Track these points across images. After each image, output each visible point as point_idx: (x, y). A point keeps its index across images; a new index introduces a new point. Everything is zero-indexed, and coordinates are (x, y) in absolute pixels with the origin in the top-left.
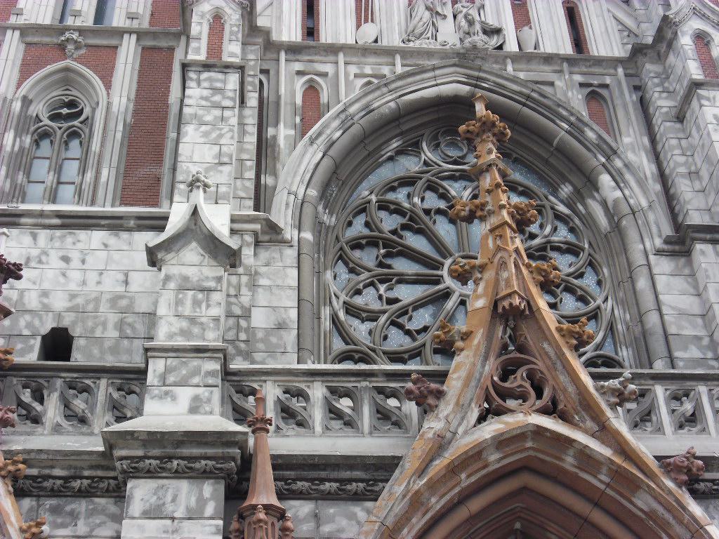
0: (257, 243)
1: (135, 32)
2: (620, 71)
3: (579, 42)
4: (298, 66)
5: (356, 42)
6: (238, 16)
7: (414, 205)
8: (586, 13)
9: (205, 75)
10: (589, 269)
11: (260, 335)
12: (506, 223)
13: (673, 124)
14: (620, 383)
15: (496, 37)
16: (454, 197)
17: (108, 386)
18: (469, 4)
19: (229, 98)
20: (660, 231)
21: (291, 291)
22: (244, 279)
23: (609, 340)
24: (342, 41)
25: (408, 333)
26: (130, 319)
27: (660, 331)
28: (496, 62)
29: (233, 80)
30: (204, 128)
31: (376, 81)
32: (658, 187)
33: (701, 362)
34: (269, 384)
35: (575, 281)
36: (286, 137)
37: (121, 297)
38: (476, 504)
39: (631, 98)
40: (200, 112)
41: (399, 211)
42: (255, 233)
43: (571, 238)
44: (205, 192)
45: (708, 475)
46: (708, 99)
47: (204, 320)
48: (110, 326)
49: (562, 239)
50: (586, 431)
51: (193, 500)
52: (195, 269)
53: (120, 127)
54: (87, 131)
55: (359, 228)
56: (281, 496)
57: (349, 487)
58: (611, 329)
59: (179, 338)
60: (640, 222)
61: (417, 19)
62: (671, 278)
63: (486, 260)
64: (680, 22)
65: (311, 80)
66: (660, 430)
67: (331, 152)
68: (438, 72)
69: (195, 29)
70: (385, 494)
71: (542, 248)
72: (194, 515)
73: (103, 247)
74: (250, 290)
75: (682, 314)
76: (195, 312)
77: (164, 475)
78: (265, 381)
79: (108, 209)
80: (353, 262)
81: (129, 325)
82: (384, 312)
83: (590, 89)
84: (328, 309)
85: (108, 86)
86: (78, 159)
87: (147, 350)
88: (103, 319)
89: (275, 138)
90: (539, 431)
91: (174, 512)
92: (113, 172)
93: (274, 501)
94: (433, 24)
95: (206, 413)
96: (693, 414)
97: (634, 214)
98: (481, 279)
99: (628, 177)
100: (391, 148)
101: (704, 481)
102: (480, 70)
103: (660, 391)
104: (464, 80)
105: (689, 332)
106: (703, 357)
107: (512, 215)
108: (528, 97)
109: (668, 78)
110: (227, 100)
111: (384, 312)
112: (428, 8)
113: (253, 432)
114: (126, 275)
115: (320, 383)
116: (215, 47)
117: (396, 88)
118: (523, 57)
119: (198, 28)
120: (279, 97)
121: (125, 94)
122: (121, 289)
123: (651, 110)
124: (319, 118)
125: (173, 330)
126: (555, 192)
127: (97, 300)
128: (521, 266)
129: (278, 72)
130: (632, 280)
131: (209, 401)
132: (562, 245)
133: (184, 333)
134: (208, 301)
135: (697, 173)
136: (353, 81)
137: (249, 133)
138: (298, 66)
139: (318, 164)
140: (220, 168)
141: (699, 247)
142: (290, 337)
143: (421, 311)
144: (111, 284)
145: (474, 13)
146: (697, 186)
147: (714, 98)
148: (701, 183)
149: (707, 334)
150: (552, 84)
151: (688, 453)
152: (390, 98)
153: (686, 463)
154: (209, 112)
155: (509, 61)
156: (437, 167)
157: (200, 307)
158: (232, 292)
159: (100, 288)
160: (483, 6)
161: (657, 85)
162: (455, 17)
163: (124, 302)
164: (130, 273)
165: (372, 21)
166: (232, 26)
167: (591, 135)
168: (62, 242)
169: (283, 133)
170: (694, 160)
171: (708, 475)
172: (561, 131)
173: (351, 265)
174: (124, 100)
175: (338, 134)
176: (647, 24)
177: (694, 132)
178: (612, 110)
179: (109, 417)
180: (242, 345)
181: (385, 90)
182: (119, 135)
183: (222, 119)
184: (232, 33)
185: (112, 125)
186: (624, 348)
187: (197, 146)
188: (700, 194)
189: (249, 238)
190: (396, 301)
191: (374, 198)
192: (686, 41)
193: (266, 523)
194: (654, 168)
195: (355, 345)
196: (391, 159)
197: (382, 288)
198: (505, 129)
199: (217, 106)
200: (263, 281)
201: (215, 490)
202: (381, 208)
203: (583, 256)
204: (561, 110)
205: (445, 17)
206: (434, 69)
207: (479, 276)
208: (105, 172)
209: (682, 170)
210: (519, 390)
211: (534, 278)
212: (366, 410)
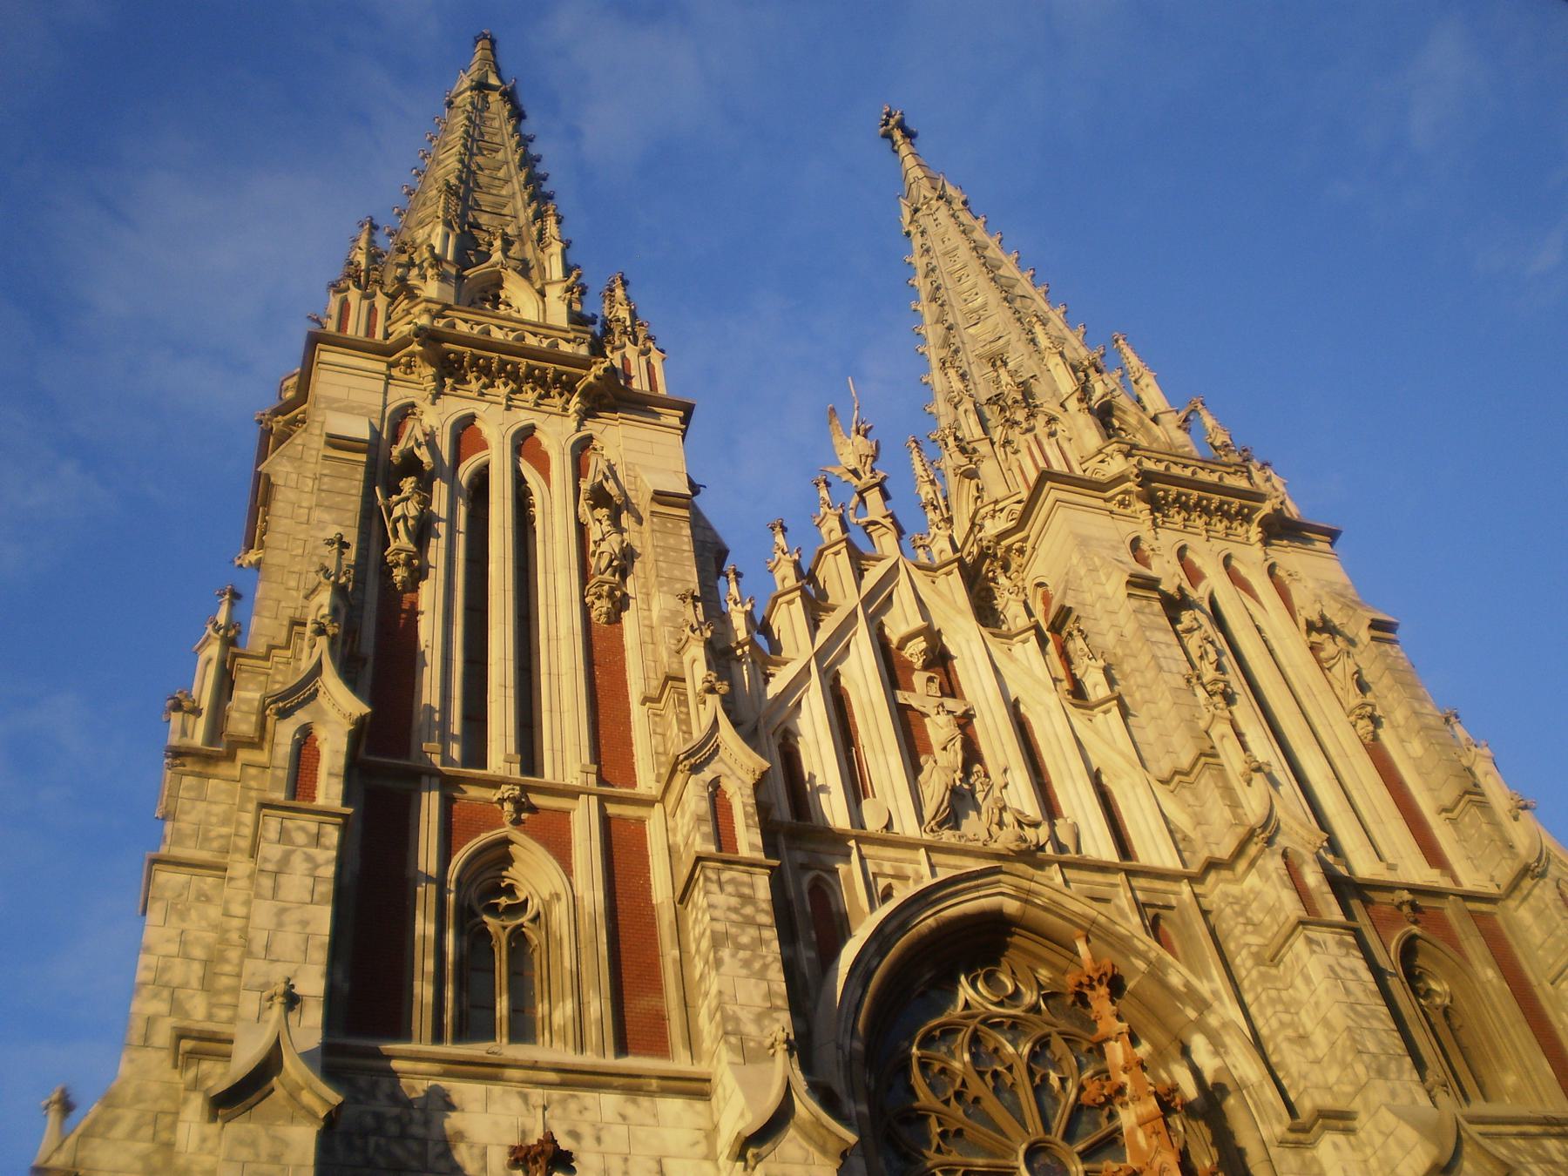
9: (726, 875)
19: (763, 911)
30: (742, 954)
36: (808, 959)
40: (733, 930)
46: (1318, 944)
73: (619, 1119)
85: (568, 869)
104: (1012, 892)
114: (660, 1162)
154: (743, 930)
164: (664, 1161)
165: (874, 796)
168: (564, 1109)
177: (1299, 982)
183: (761, 941)
188: (1316, 1067)
196: (923, 994)
199: (750, 922)
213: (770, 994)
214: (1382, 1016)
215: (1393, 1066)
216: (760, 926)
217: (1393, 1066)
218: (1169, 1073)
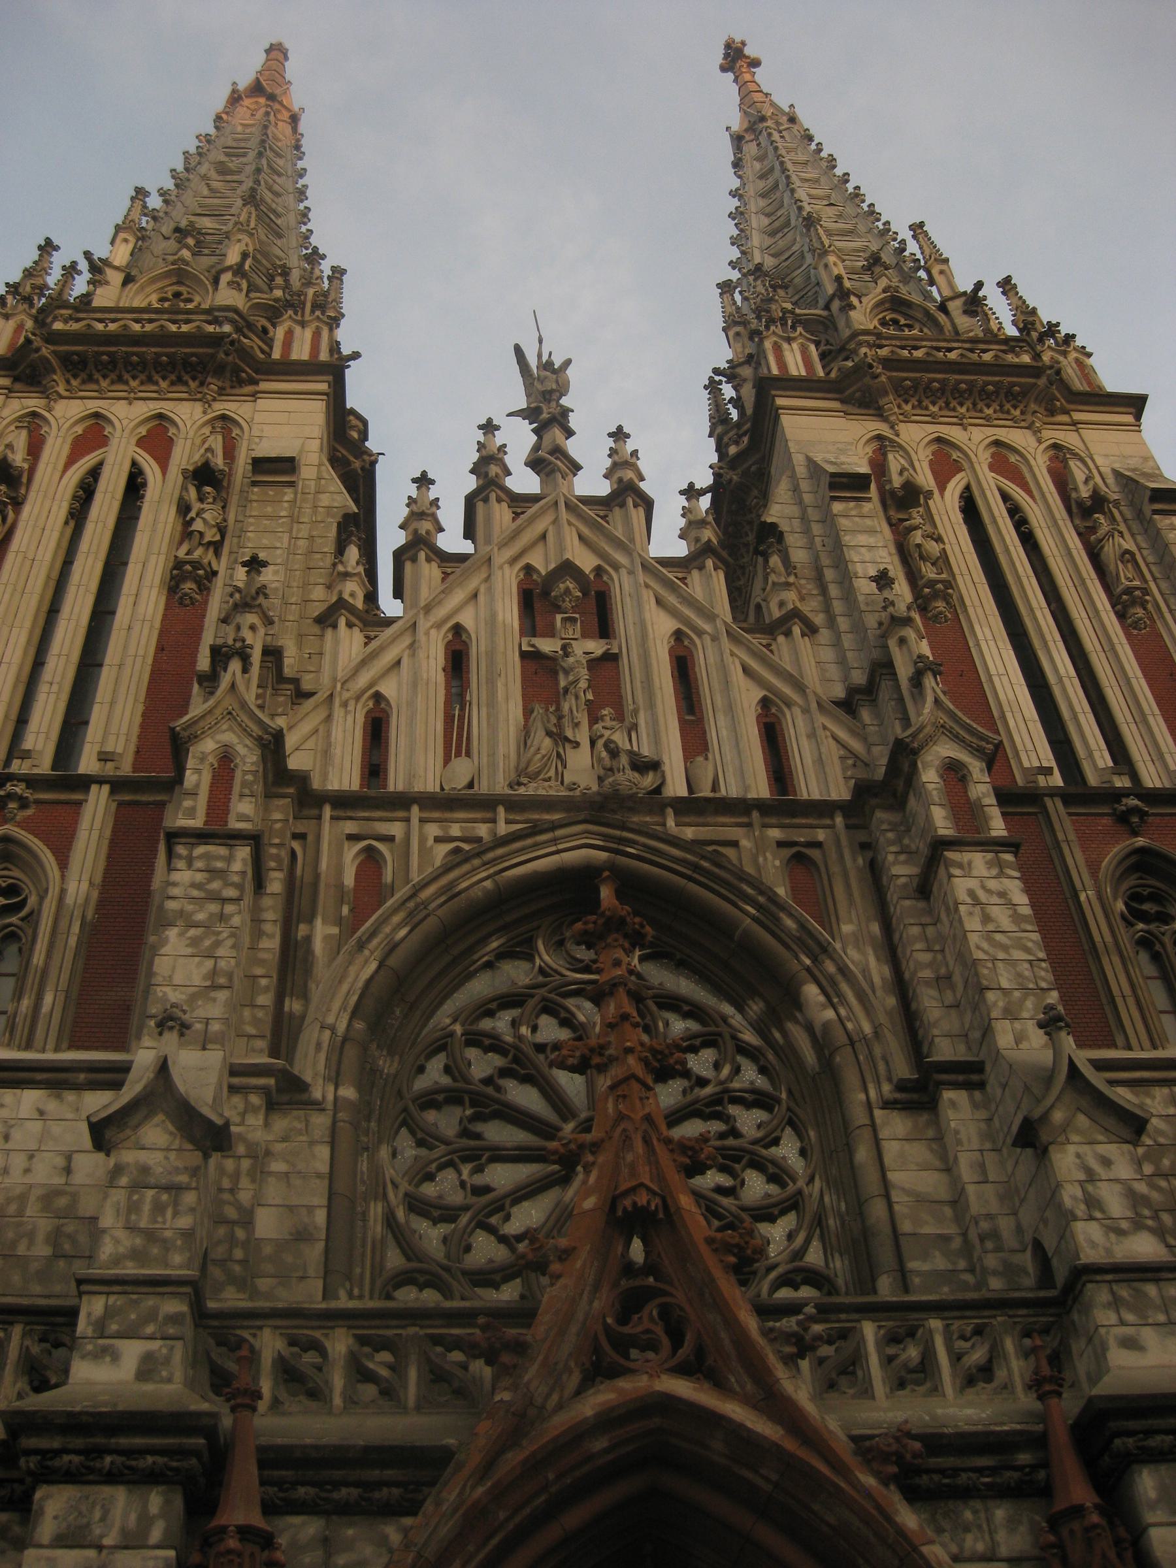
0: (272, 1106)
1: (106, 782)
2: (839, 820)
3: (780, 773)
4: (350, 827)
5: (442, 789)
6: (255, 758)
7: (520, 1038)
8: (792, 731)
9: (200, 850)
10: (788, 1131)
11: (268, 1250)
12: (633, 1076)
13: (914, 902)
14: (799, 1323)
15: (651, 775)
16: (581, 1024)
17: (24, 1335)
18: (614, 723)
19: (233, 885)
20: (889, 1071)
21: (318, 1181)
22: (246, 1164)
23: (816, 1244)
24: (418, 787)
25: (503, 1239)
26: (70, 1228)
27: (886, 1229)
28: (651, 812)
30: (192, 932)
31: (466, 847)
32: (891, 1001)
33: (948, 1276)
34: (267, 1334)
35: (764, 1152)
36: (327, 938)
37: (56, 1193)
38: (574, 1518)
39: (855, 863)
40: (190, 908)
41: (493, 1045)
42: (265, 1091)
43: (761, 1082)
44: (182, 1035)
45: (934, 1462)
46: (960, 866)
47: (168, 1234)
48: (40, 1237)
49: (746, 1085)
50: (746, 1400)
51: (133, 1517)
52: (159, 1156)
53: (76, 928)
54: (30, 932)
55: (435, 1074)
56: (270, 1509)
57: (377, 1495)
58: (820, 1224)
59: (130, 1264)
60: (861, 1058)
61: (532, 750)
62: (907, 1146)
63: (602, 1135)
64: (921, 747)
65: (369, 850)
66: (867, 1392)
67: (392, 961)
68: (560, 833)
69: (190, 778)
70: (429, 1506)
71: (716, 1100)
72: (132, 1541)
74: (253, 1181)
75: (921, 1200)
76: (156, 1222)
77: (91, 1477)
78: (260, 1328)
79: (50, 1056)
80: (422, 1130)
81: (69, 1236)
82: (466, 1208)
84: (380, 1205)
85: (63, 864)
86: (13, 975)
87: (80, 1282)
88: (30, 1227)
89: (308, 939)
90: (668, 1404)
91: (102, 1537)
92: (61, 997)
93: (256, 1519)
94: (559, 755)
95: (162, 1381)
96: (922, 1362)
97: (852, 1043)
98: (593, 1163)
99: (845, 987)
100: (488, 949)
101: (928, 1471)
102: (623, 828)
103: (869, 1330)
105: (927, 1230)
106: (950, 1267)
107: (646, 1062)
108: (696, 868)
109: (908, 830)
111: (466, 1208)
112: (549, 734)
113: (233, 1409)
114: (69, 1158)
115: (344, 1330)
116: (219, 805)
117: (495, 859)
118: (689, 807)
119: (195, 777)
120: (317, 876)
121: (86, 877)
122: (58, 1180)
123: (885, 880)
124: (379, 906)
125: (121, 1250)
126: (740, 1009)
127: (23, 1198)
128: (655, 1142)
129: (318, 837)
130: (850, 1150)
131: (167, 1361)
132: (746, 1095)
133: (136, 1255)
134: (176, 1204)
135: (949, 977)
136: (431, 848)
137: (268, 935)
138: (350, 827)
139: (369, 982)
140: (213, 994)
141: (948, 1095)
142: (314, 1253)
143: (525, 1204)
144: (45, 1173)
145: (619, 738)
146: (949, 998)
147: (970, 863)
148: (954, 991)
149: (958, 1231)
150: (735, 844)
151: (899, 1430)
152: (484, 874)
153: (894, 1447)
154: (201, 909)
155: (670, 811)
156: (558, 977)
157: (163, 1215)
158: (226, 1183)
159: (29, 1179)
160: (635, 727)
161: (893, 843)
162: (593, 743)
163: (62, 1202)
164: (75, 1156)
165: (468, 754)
166: (245, 773)
167: (789, 923)
169: (321, 932)
170: (944, 957)
171: (934, 1462)
172: (745, 917)
173: (420, 1135)
174: (85, 885)
175: (403, 932)
176: (879, 748)
177: (943, 916)
178: (826, 882)
179: (22, 1384)
180: (237, 1268)
181: (476, 862)
182: (73, 941)
184: (244, 784)
185: (63, 924)
186: (837, 1256)
187: (181, 960)
188: (953, 1012)
189: (255, 1099)
190: (487, 1189)
191: (458, 1029)
192: (930, 777)
193: (240, 1555)
194: (886, 970)
195: (421, 1262)
197: (466, 1170)
198: (642, 926)
200: (277, 1166)
201: (167, 1502)
202: (470, 1043)
203: (781, 1110)
204: (745, 887)
205: (577, 745)
206: (554, 827)
207: (590, 1158)
208: (48, 999)
209: (927, 974)
210: (645, 1337)
211: (675, 1161)
212: (413, 1374)
213: (214, 972)
214: (1030, 944)
215: (1029, 1004)
216: (224, 901)
217: (1029, 1004)
218: (785, 1034)
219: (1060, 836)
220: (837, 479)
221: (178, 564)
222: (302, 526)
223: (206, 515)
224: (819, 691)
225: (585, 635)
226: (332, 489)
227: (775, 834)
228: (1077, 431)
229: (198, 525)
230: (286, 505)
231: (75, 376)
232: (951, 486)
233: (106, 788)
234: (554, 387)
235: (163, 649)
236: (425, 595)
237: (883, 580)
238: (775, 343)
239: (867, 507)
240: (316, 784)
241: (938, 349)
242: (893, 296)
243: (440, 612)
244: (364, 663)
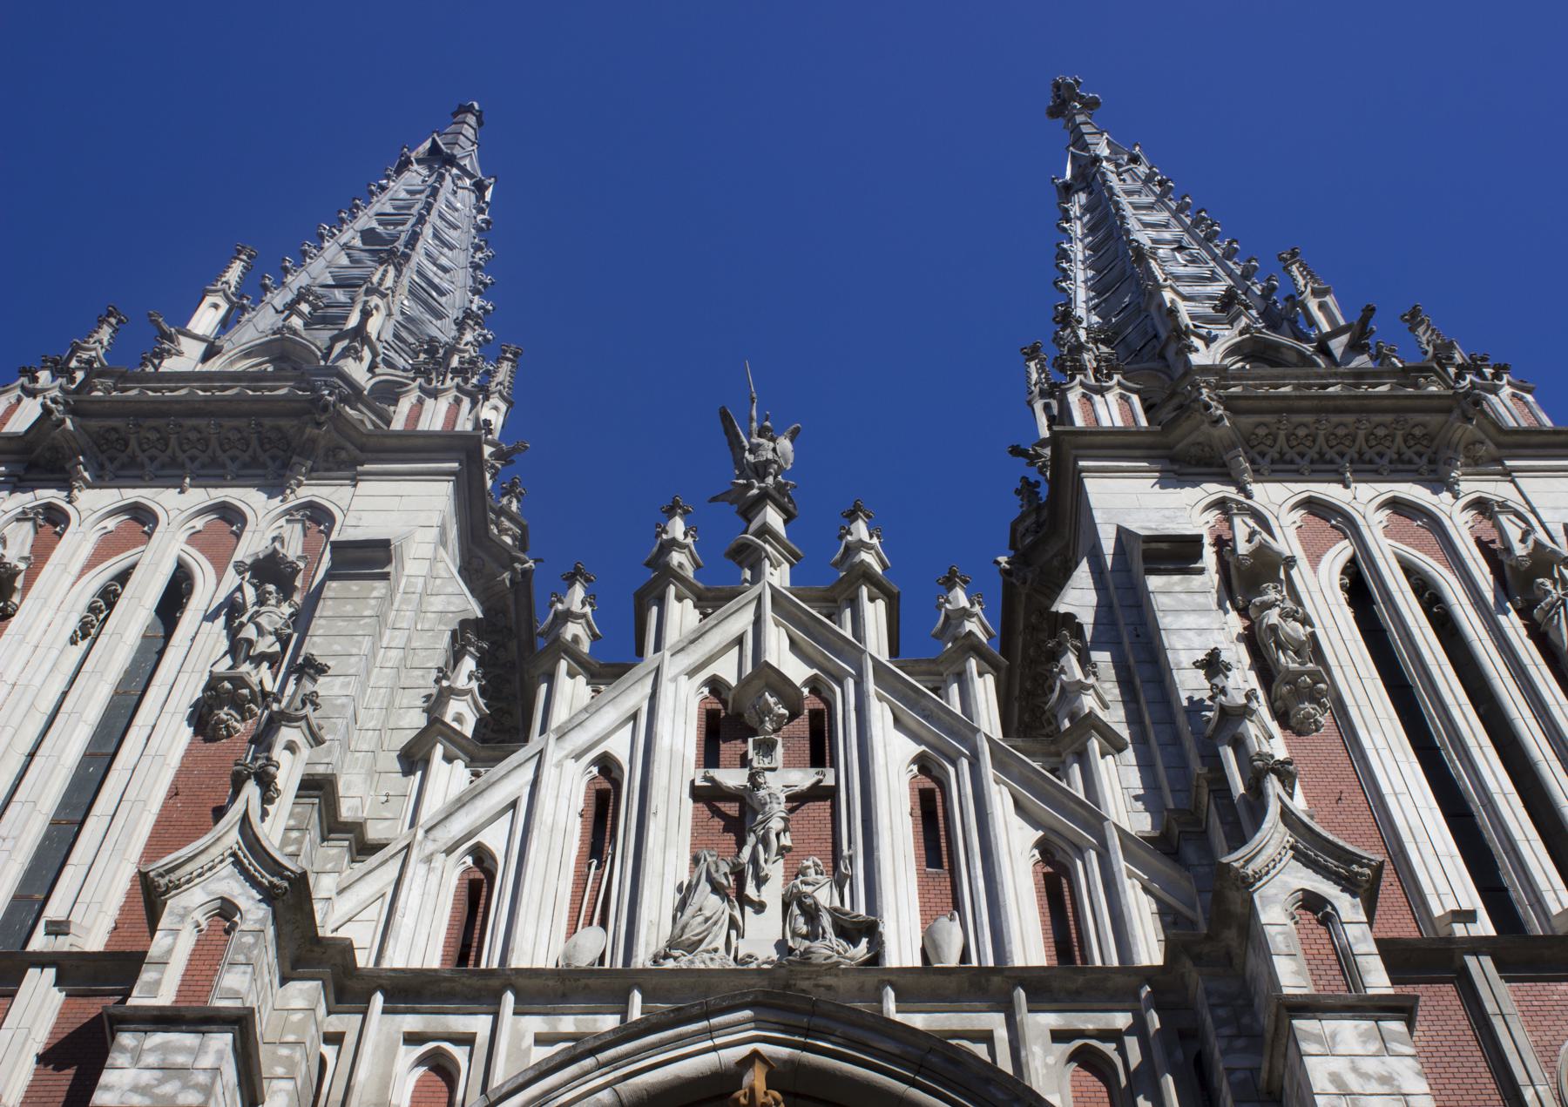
4: (412, 1023)
9: (158, 1038)
24: (518, 961)
29: (222, 1042)
46: (1318, 1039)
68: (714, 1021)
83: (1078, 1043)
94: (733, 923)
110: (191, 1091)
112: (717, 889)
136: (529, 1049)
145: (825, 896)
147: (1334, 1036)
162: (786, 906)
165: (604, 923)
181: (589, 1062)
205: (760, 907)
219: (1490, 1007)
220: (1154, 545)
221: (213, 683)
222: (397, 633)
223: (262, 620)
224: (1126, 826)
225: (788, 764)
226: (450, 590)
227: (1051, 1020)
228: (1512, 481)
229: (250, 632)
230: (373, 602)
231: (112, 460)
232: (1327, 558)
233: (50, 973)
234: (770, 456)
235: (176, 794)
236: (560, 715)
237: (1213, 665)
238: (1084, 395)
239: (1196, 581)
240: (364, 960)
241: (1309, 387)
242: (1253, 338)
243: (579, 739)
244: (461, 803)
